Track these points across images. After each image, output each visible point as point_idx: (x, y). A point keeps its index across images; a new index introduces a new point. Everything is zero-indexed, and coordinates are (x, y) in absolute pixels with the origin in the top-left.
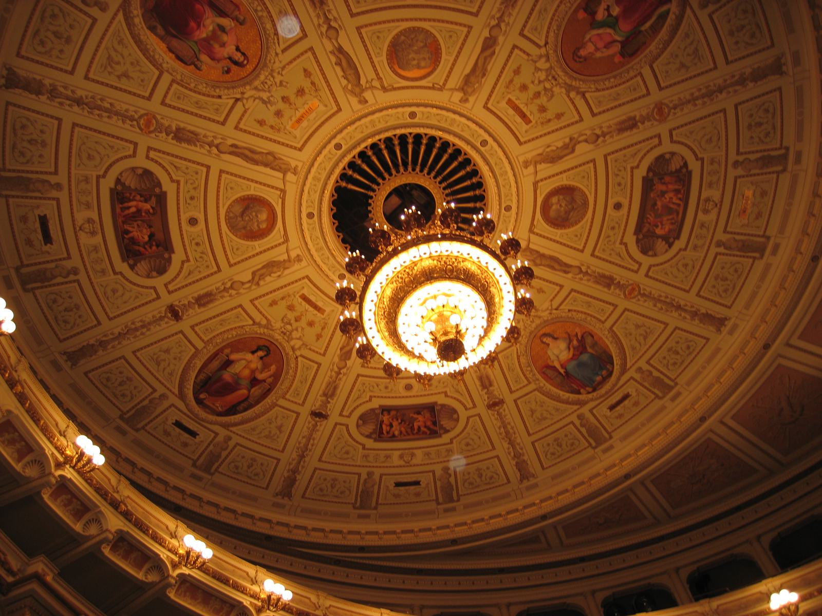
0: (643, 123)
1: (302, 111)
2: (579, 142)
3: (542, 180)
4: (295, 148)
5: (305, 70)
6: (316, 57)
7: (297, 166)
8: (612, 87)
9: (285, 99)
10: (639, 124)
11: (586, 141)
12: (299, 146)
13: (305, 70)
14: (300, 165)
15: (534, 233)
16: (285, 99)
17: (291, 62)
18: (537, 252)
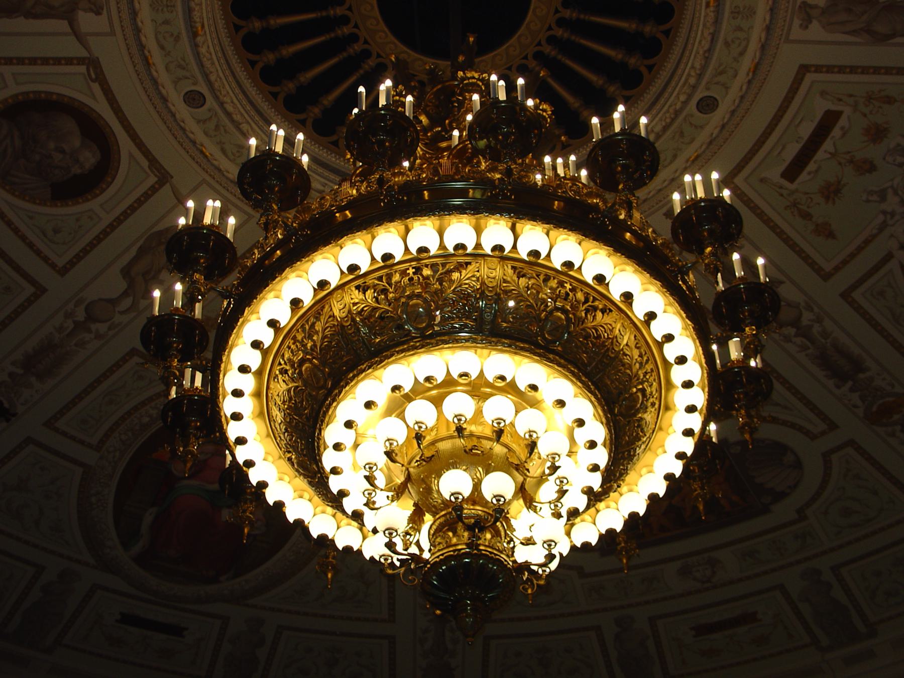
0: (11, 375)
1: (820, 155)
2: (125, 294)
3: (154, 190)
4: (818, 69)
5: (831, 235)
6: (812, 264)
7: (805, 26)
8: (136, 408)
9: (867, 167)
10: (20, 371)
11: (114, 302)
12: (809, 78)
13: (831, 235)
14: (797, 32)
15: (80, 61)
16: (867, 167)
17: (867, 242)
18: (36, 16)
